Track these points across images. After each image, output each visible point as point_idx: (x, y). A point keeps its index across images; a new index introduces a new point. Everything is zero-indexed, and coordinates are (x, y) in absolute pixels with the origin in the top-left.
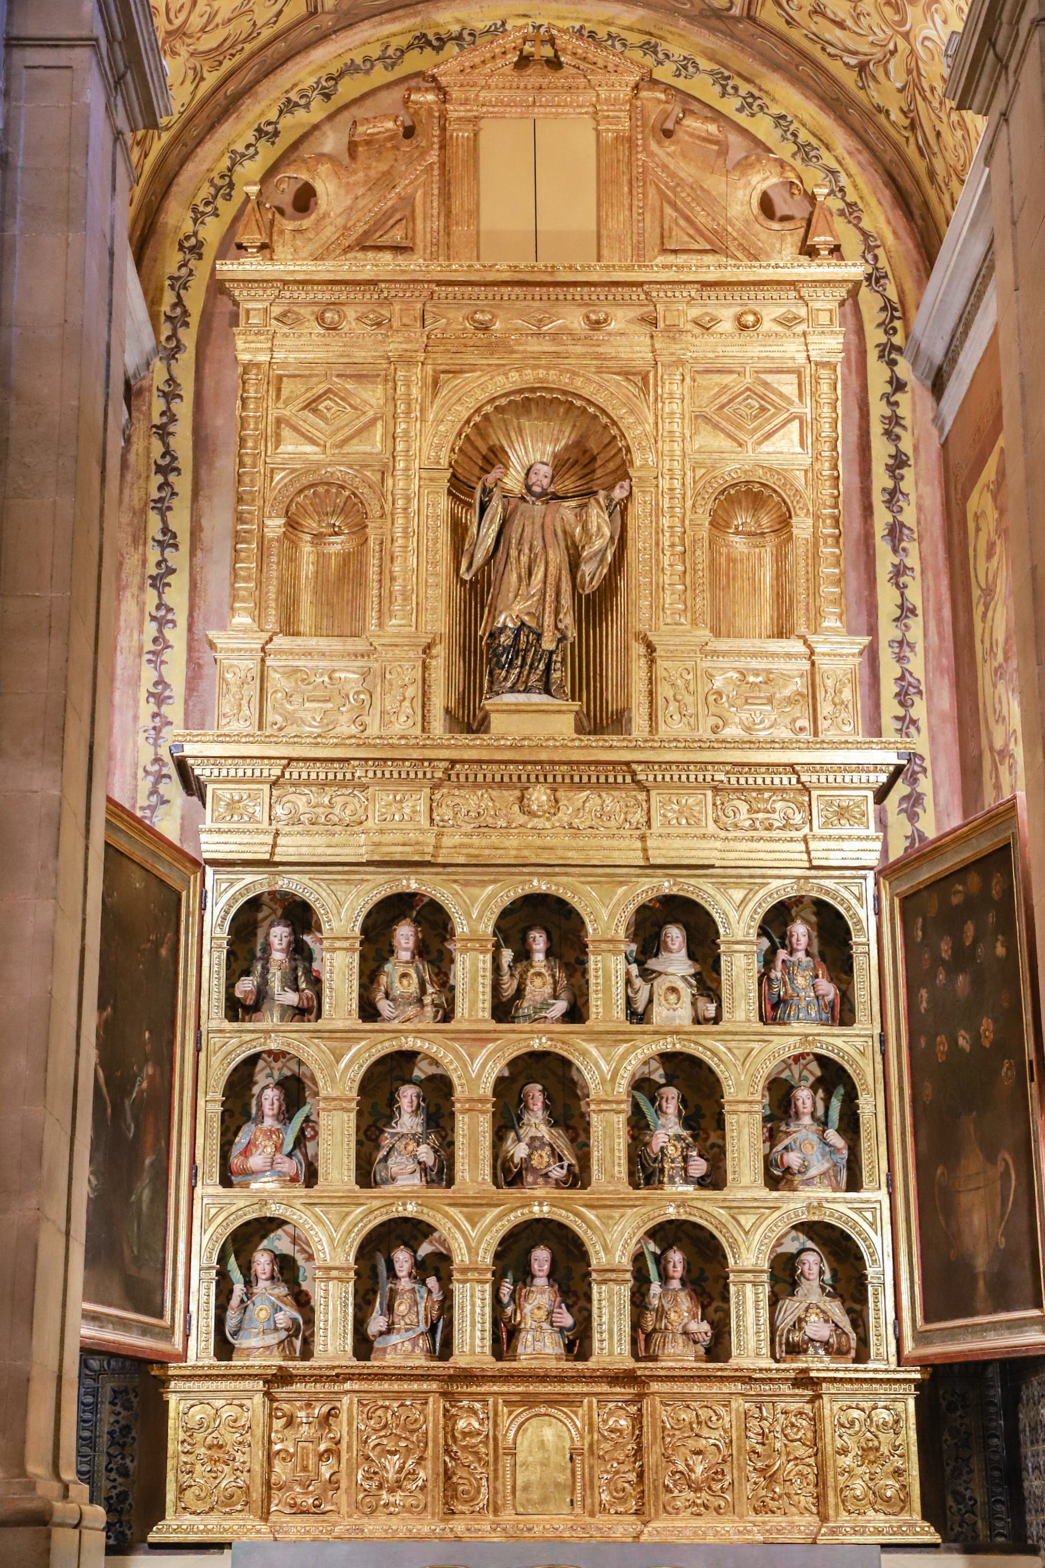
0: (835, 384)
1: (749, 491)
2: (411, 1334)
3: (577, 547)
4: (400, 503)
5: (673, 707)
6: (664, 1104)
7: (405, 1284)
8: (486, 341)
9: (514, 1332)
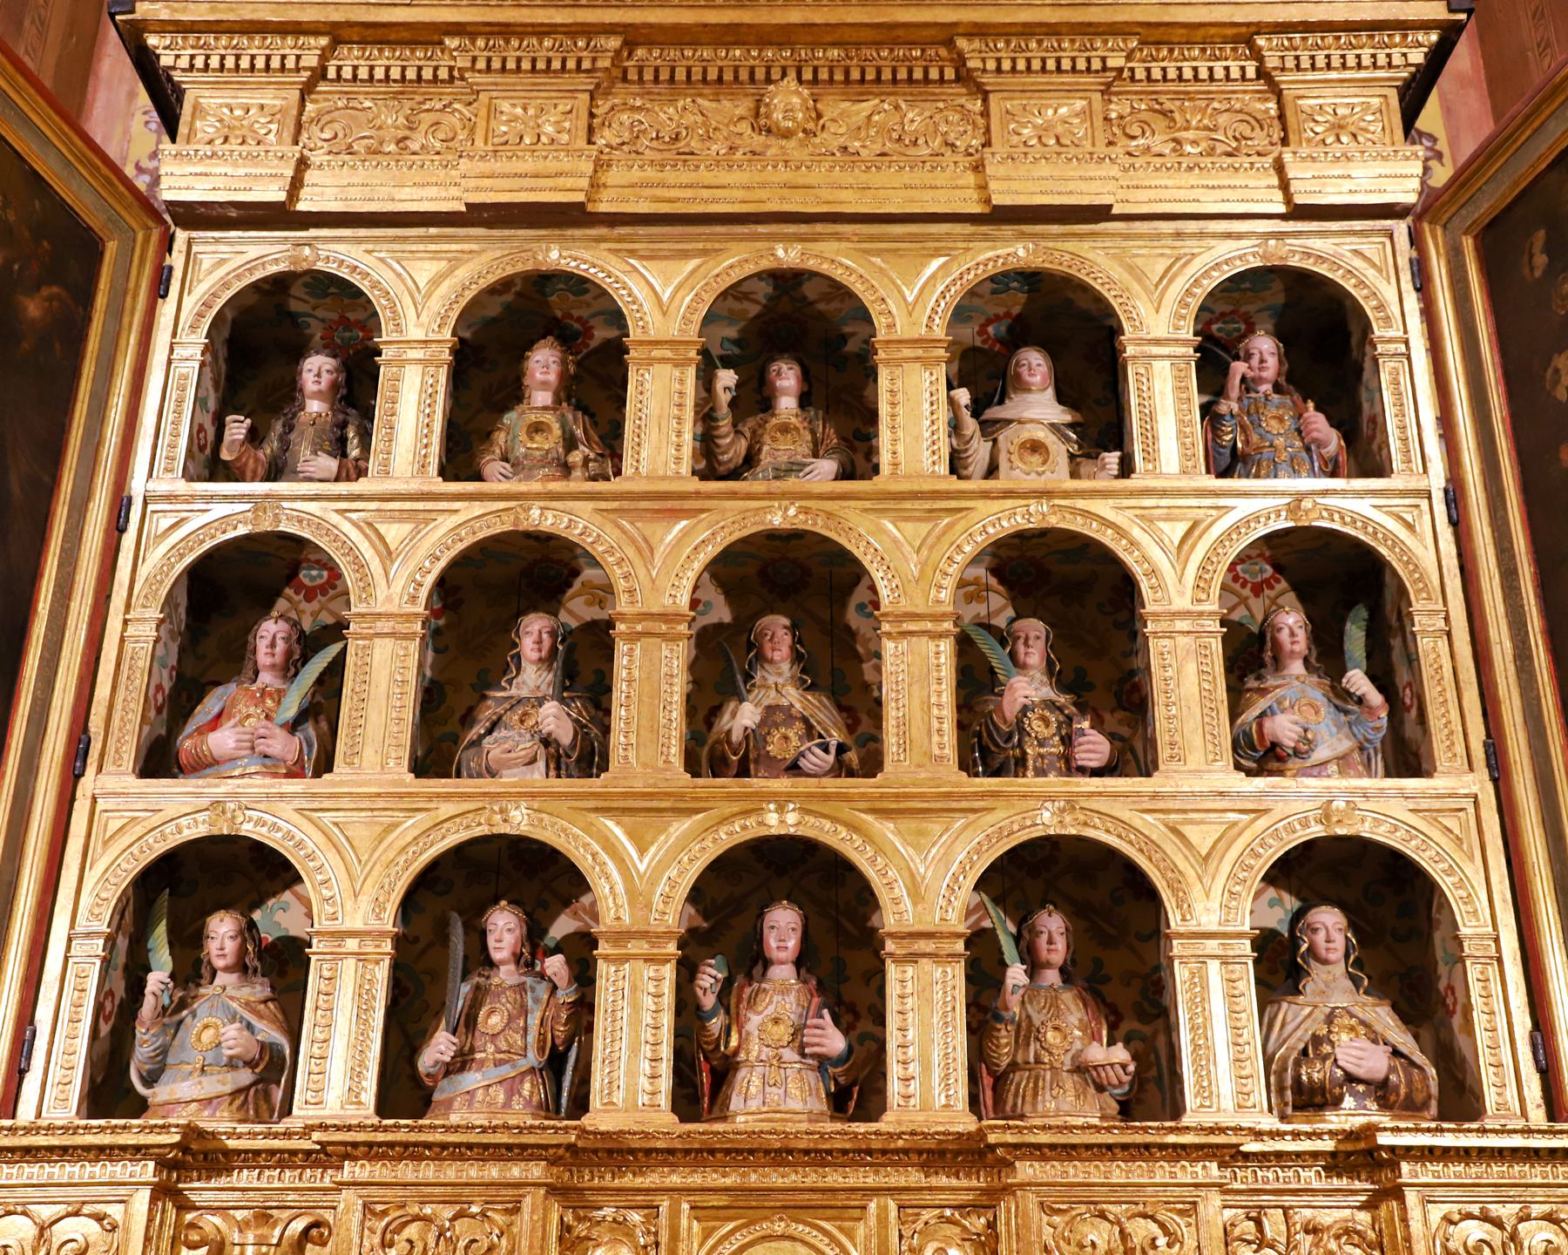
2: (506, 1071)
6: (1021, 649)
7: (507, 975)
9: (725, 1071)
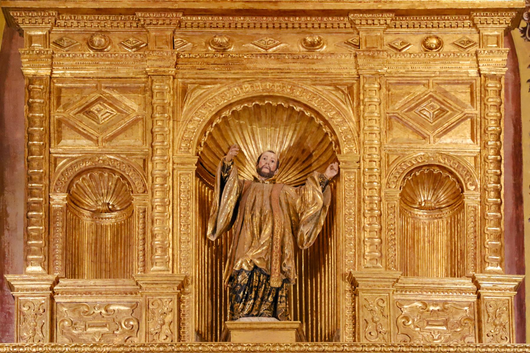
0: (500, 91)
1: (431, 173)
3: (297, 214)
4: (158, 181)
5: (370, 327)
8: (224, 60)
